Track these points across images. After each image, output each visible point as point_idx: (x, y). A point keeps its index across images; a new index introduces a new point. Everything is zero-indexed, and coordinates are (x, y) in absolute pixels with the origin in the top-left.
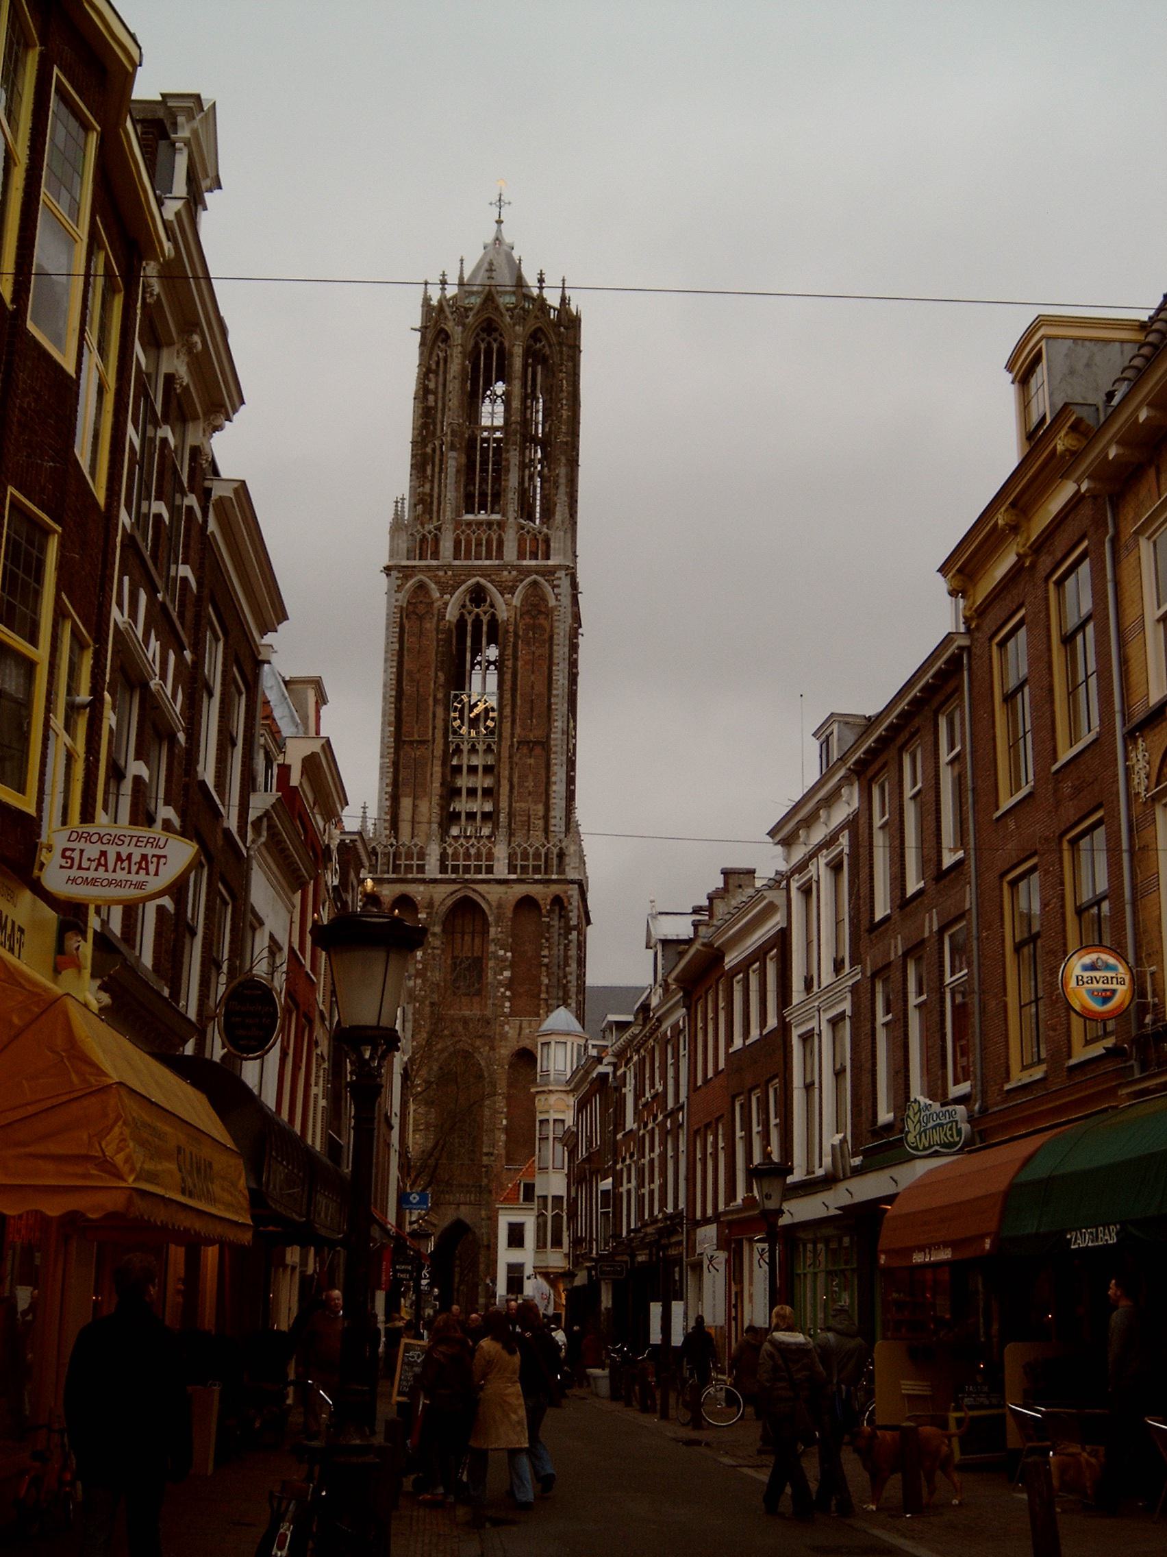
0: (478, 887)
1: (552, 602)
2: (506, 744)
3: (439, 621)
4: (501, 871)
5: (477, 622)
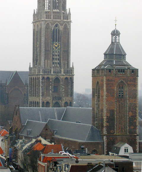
0: (59, 76)
1: (68, 27)
2: (62, 52)
3: (51, 30)
4: (62, 72)
5: (56, 30)
